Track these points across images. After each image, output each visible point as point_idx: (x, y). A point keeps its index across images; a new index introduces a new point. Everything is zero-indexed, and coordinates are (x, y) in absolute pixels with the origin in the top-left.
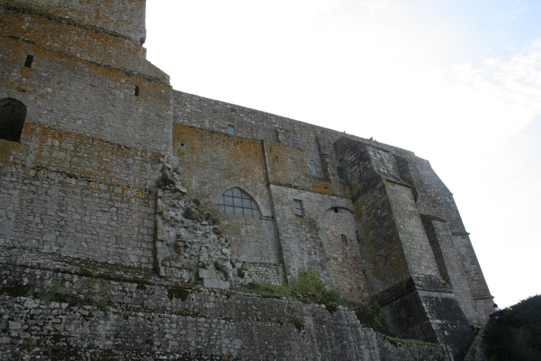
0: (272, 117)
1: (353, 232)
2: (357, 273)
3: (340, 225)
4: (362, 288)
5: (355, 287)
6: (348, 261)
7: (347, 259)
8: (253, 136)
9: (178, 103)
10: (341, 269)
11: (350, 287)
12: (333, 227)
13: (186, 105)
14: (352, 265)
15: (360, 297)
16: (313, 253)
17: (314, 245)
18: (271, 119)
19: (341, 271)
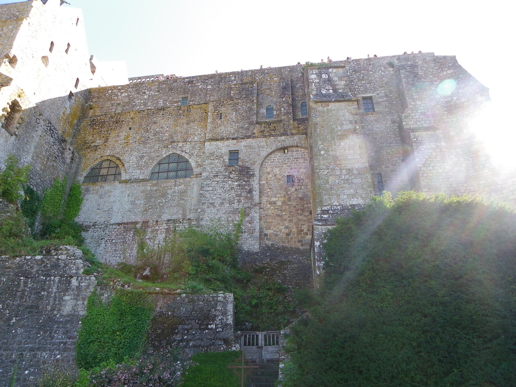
0: (231, 76)
1: (304, 171)
2: (301, 215)
3: (287, 166)
4: (305, 230)
5: (294, 230)
6: (290, 203)
7: (290, 201)
8: (206, 101)
9: (138, 94)
10: (279, 212)
11: (287, 231)
12: (277, 169)
13: (144, 93)
14: (295, 207)
15: (300, 241)
16: (236, 201)
17: (239, 193)
18: (230, 77)
19: (278, 215)
